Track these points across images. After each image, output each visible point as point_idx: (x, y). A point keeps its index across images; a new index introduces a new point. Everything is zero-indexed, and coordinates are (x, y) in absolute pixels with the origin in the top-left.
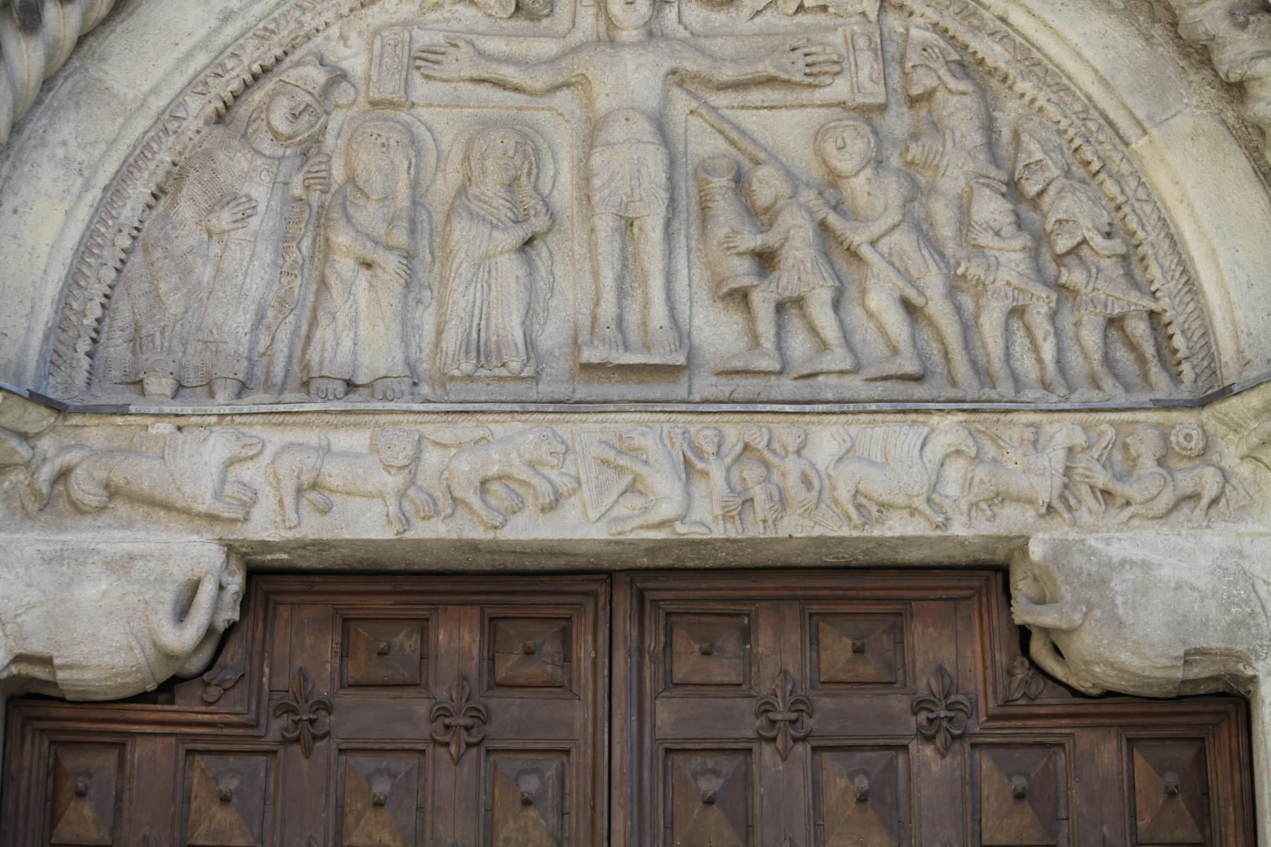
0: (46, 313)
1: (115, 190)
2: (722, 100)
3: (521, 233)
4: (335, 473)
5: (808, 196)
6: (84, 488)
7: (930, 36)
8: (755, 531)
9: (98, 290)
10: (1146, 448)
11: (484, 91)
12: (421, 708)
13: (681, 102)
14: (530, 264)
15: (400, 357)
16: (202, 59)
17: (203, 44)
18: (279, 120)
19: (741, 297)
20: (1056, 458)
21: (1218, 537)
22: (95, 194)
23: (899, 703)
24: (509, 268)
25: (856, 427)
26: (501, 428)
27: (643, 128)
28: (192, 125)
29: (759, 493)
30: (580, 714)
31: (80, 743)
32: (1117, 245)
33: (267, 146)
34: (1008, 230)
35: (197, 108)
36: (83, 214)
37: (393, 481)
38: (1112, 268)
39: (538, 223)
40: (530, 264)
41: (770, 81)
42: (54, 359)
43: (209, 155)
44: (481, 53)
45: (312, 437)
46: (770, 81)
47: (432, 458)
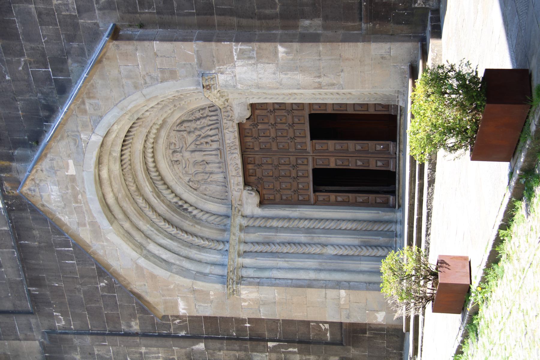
0: (220, 205)
1: (206, 199)
2: (188, 145)
3: (206, 164)
4: (236, 182)
5: (199, 139)
6: (240, 203)
7: (178, 127)
8: (238, 147)
9: (217, 200)
10: (226, 114)
11: (190, 167)
12: (258, 170)
13: (188, 149)
14: (210, 163)
15: (221, 174)
16: (190, 193)
17: (188, 193)
18: (196, 186)
19: (211, 145)
20: (228, 122)
21: (234, 106)
22: (207, 201)
23: (254, 129)
24: (210, 165)
25: (226, 139)
26: (230, 169)
27: (193, 154)
28: (197, 193)
29: (234, 147)
30: (257, 156)
31: (264, 197)
32: (201, 111)
33: (199, 186)
34: (200, 121)
35: (195, 192)
36: (209, 202)
37: (236, 178)
38: (203, 111)
39: (205, 162)
40: (210, 163)
41: (185, 142)
42: (225, 204)
43: (201, 191)
44: (185, 167)
45: (232, 184)
46: (185, 142)
47: (233, 174)
